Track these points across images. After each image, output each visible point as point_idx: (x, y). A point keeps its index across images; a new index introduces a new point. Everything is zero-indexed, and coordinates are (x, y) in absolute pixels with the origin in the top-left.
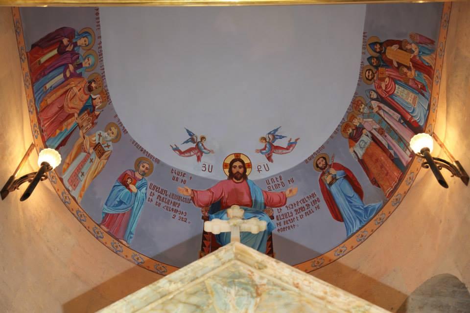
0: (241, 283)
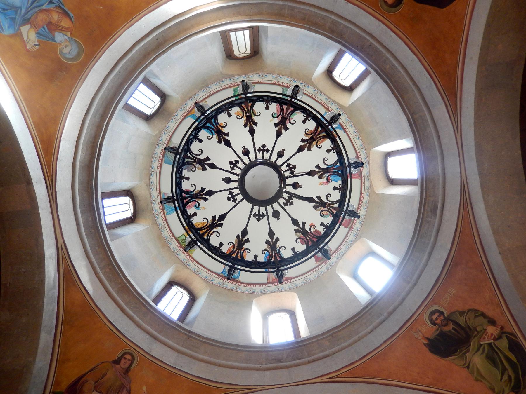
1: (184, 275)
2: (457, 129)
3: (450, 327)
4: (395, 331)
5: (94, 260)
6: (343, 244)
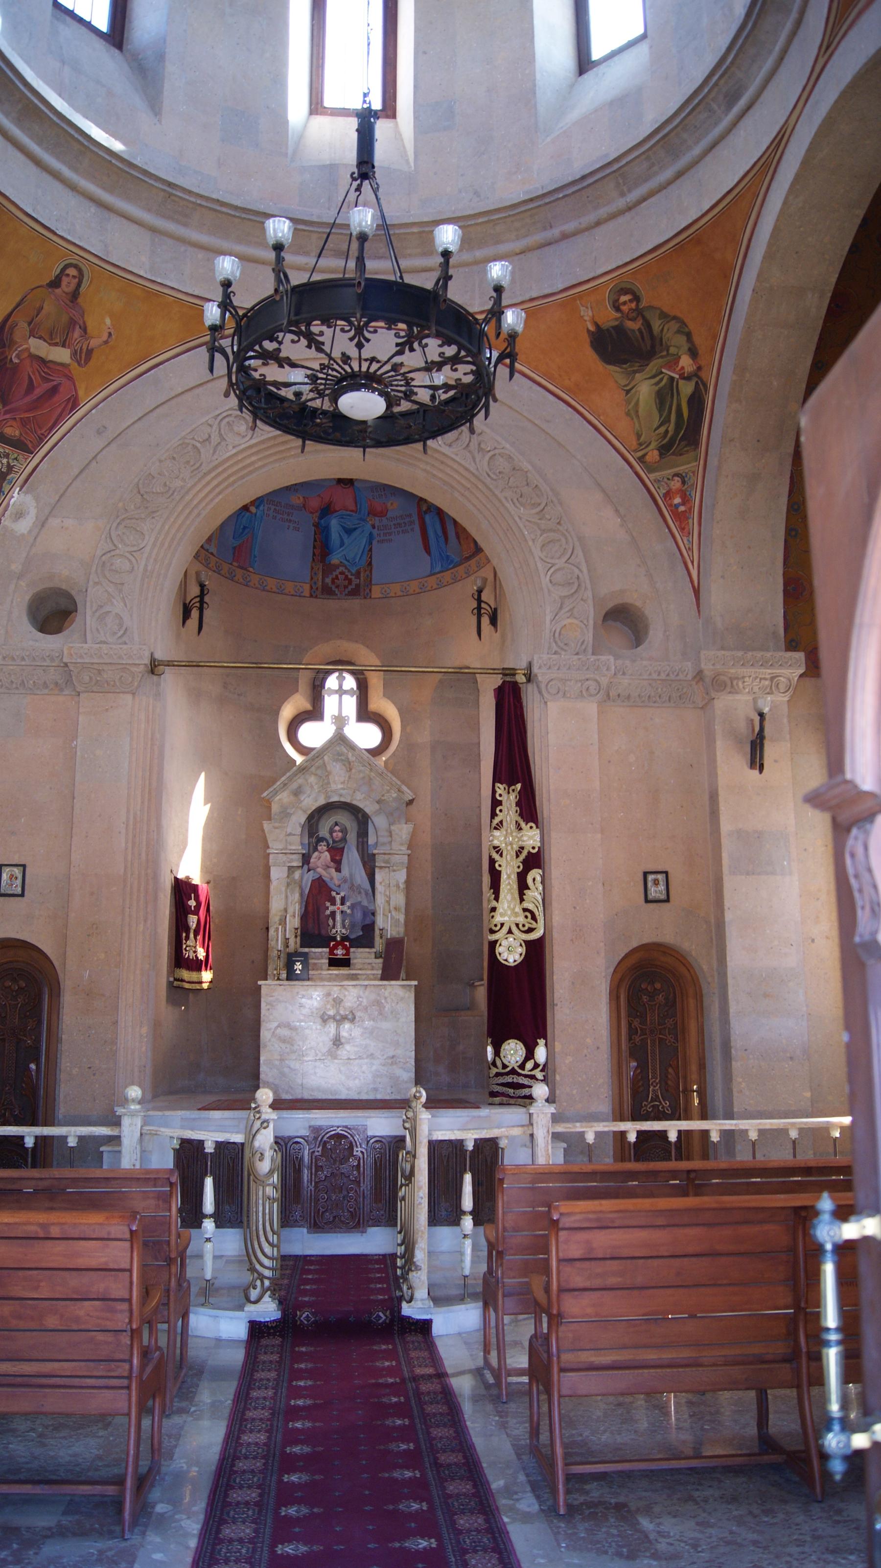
0: (342, 760)
2: (828, 47)
3: (634, 326)
4: (555, 290)
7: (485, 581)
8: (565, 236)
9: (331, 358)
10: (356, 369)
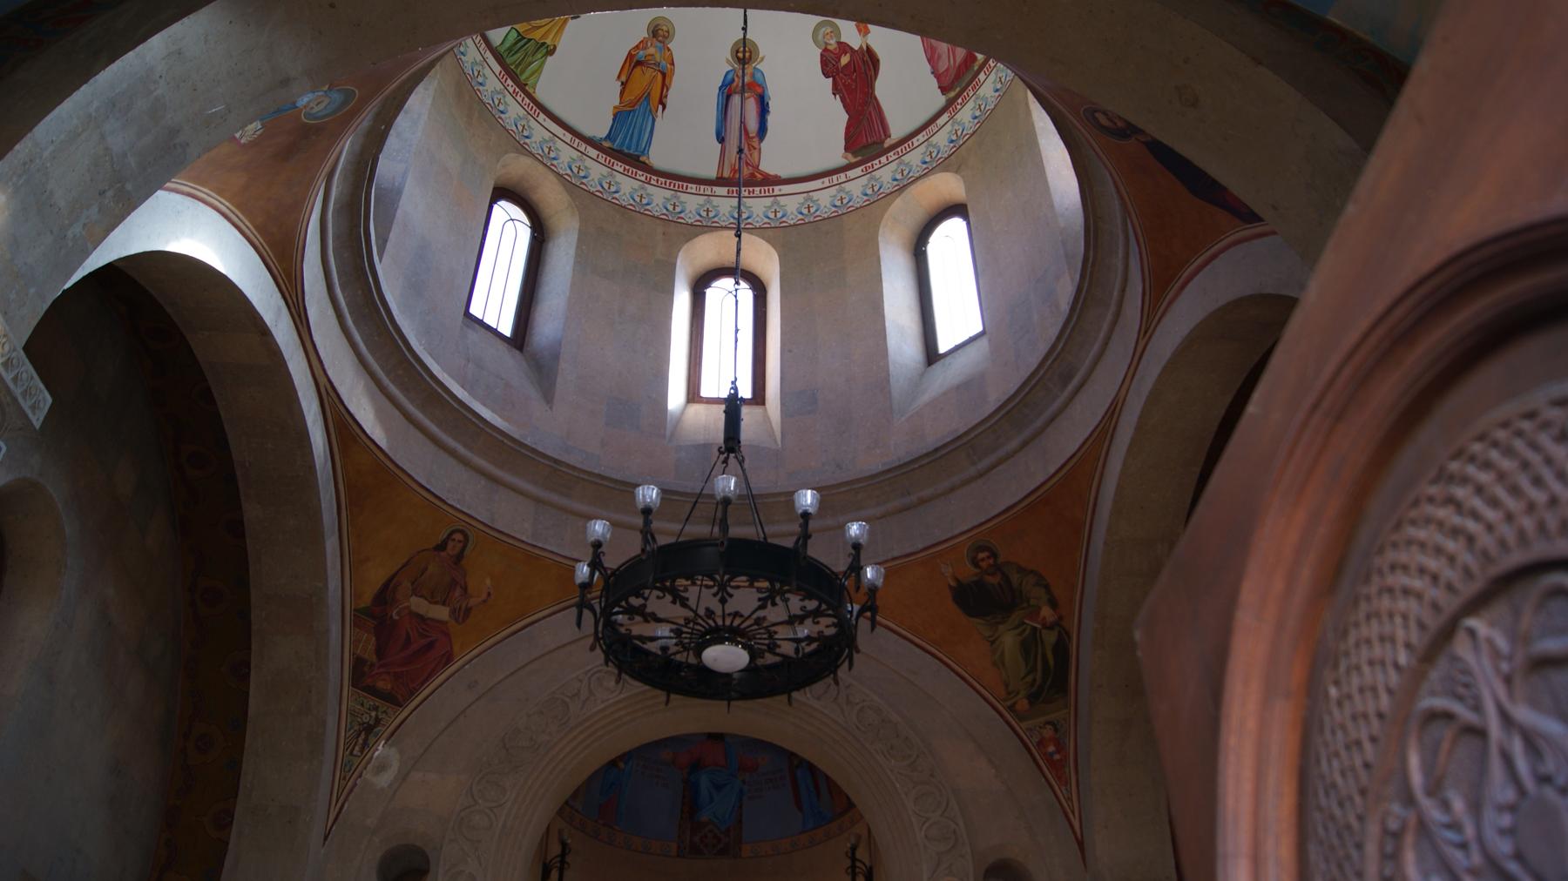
1: (516, 167)
2: (1146, 331)
3: (993, 580)
5: (376, 367)
6: (921, 137)
7: (859, 837)
8: (922, 502)
9: (695, 612)
10: (720, 622)
